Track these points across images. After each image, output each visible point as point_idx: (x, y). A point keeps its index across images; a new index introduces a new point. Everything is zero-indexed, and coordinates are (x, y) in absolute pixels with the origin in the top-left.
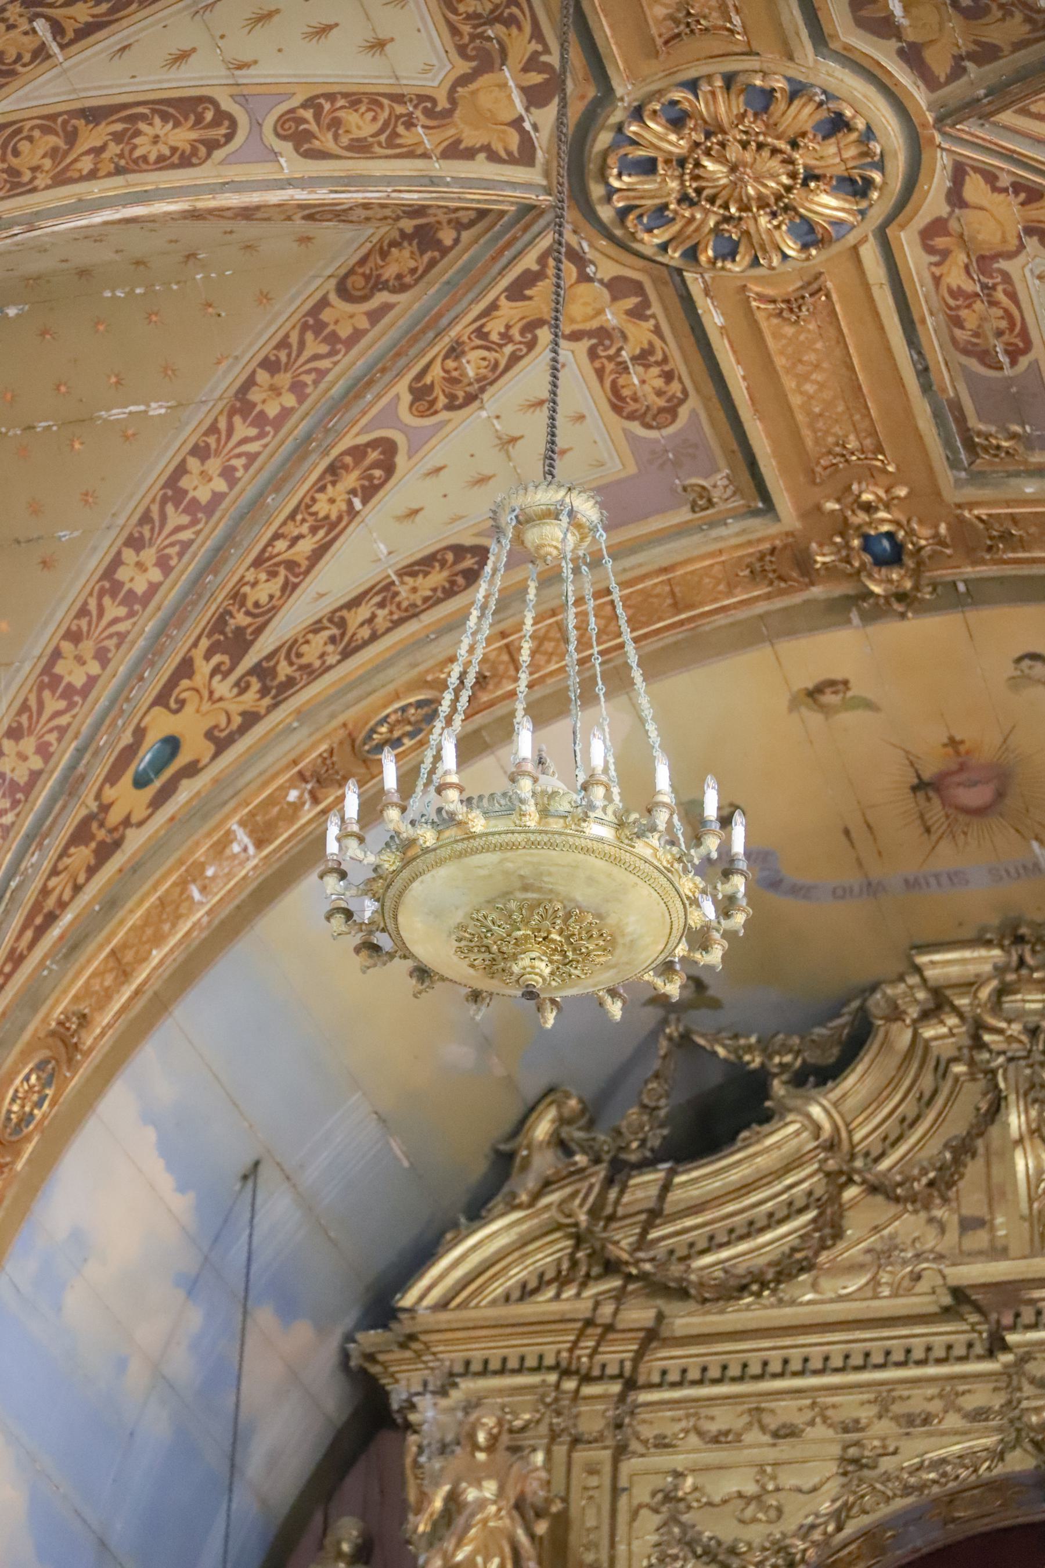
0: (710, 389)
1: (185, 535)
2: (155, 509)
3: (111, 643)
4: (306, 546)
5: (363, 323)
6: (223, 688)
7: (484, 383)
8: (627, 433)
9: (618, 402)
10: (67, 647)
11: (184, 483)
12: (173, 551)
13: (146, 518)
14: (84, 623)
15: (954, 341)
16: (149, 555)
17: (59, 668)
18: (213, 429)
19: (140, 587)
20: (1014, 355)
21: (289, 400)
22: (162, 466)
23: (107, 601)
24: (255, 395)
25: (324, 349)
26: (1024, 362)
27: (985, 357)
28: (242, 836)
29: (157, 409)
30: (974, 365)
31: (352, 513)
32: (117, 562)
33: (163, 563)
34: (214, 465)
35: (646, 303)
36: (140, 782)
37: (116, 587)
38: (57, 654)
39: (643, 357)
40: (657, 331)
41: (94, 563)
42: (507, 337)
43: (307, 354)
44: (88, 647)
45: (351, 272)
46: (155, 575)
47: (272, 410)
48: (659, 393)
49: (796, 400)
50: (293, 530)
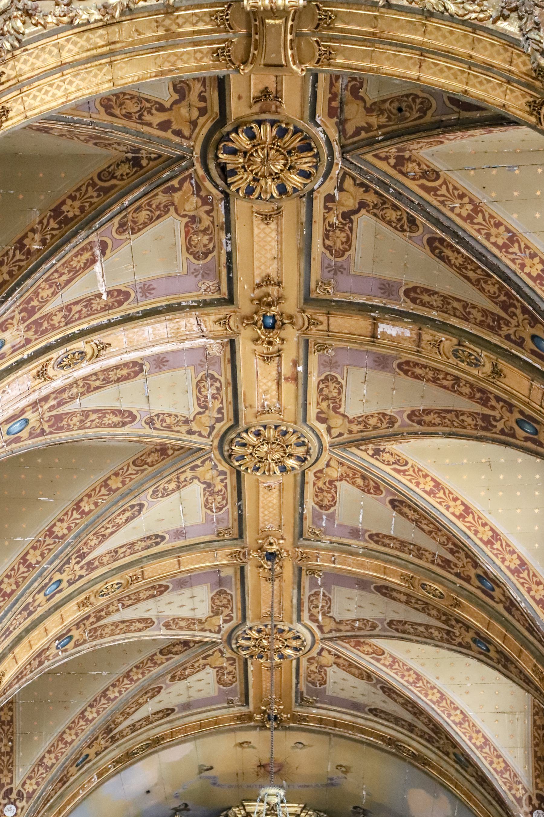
0: (243, 681)
1: (105, 706)
2: (98, 698)
3: (80, 731)
4: (133, 709)
5: (164, 661)
6: (103, 742)
7: (189, 675)
8: (219, 689)
9: (219, 682)
10: (67, 730)
11: (108, 693)
12: (101, 709)
13: (95, 700)
14: (73, 725)
15: (307, 680)
16: (94, 710)
17: (65, 736)
18: (118, 680)
19: (90, 718)
20: (321, 685)
21: (140, 676)
22: (103, 687)
23: (81, 720)
24: (131, 674)
25: (152, 665)
26: (323, 687)
27: (314, 684)
28: (96, 777)
29: (104, 673)
30: (310, 685)
31: (147, 701)
32: (85, 710)
33: (98, 713)
34: (116, 689)
35: (235, 663)
36: (77, 766)
37: (84, 717)
38: (64, 732)
39: (229, 673)
40: (235, 668)
41: (79, 710)
42: (198, 667)
43: (148, 666)
44: (73, 731)
45: (164, 649)
46: (95, 715)
47: (135, 678)
48: (230, 680)
49: (264, 686)
50: (132, 706)
